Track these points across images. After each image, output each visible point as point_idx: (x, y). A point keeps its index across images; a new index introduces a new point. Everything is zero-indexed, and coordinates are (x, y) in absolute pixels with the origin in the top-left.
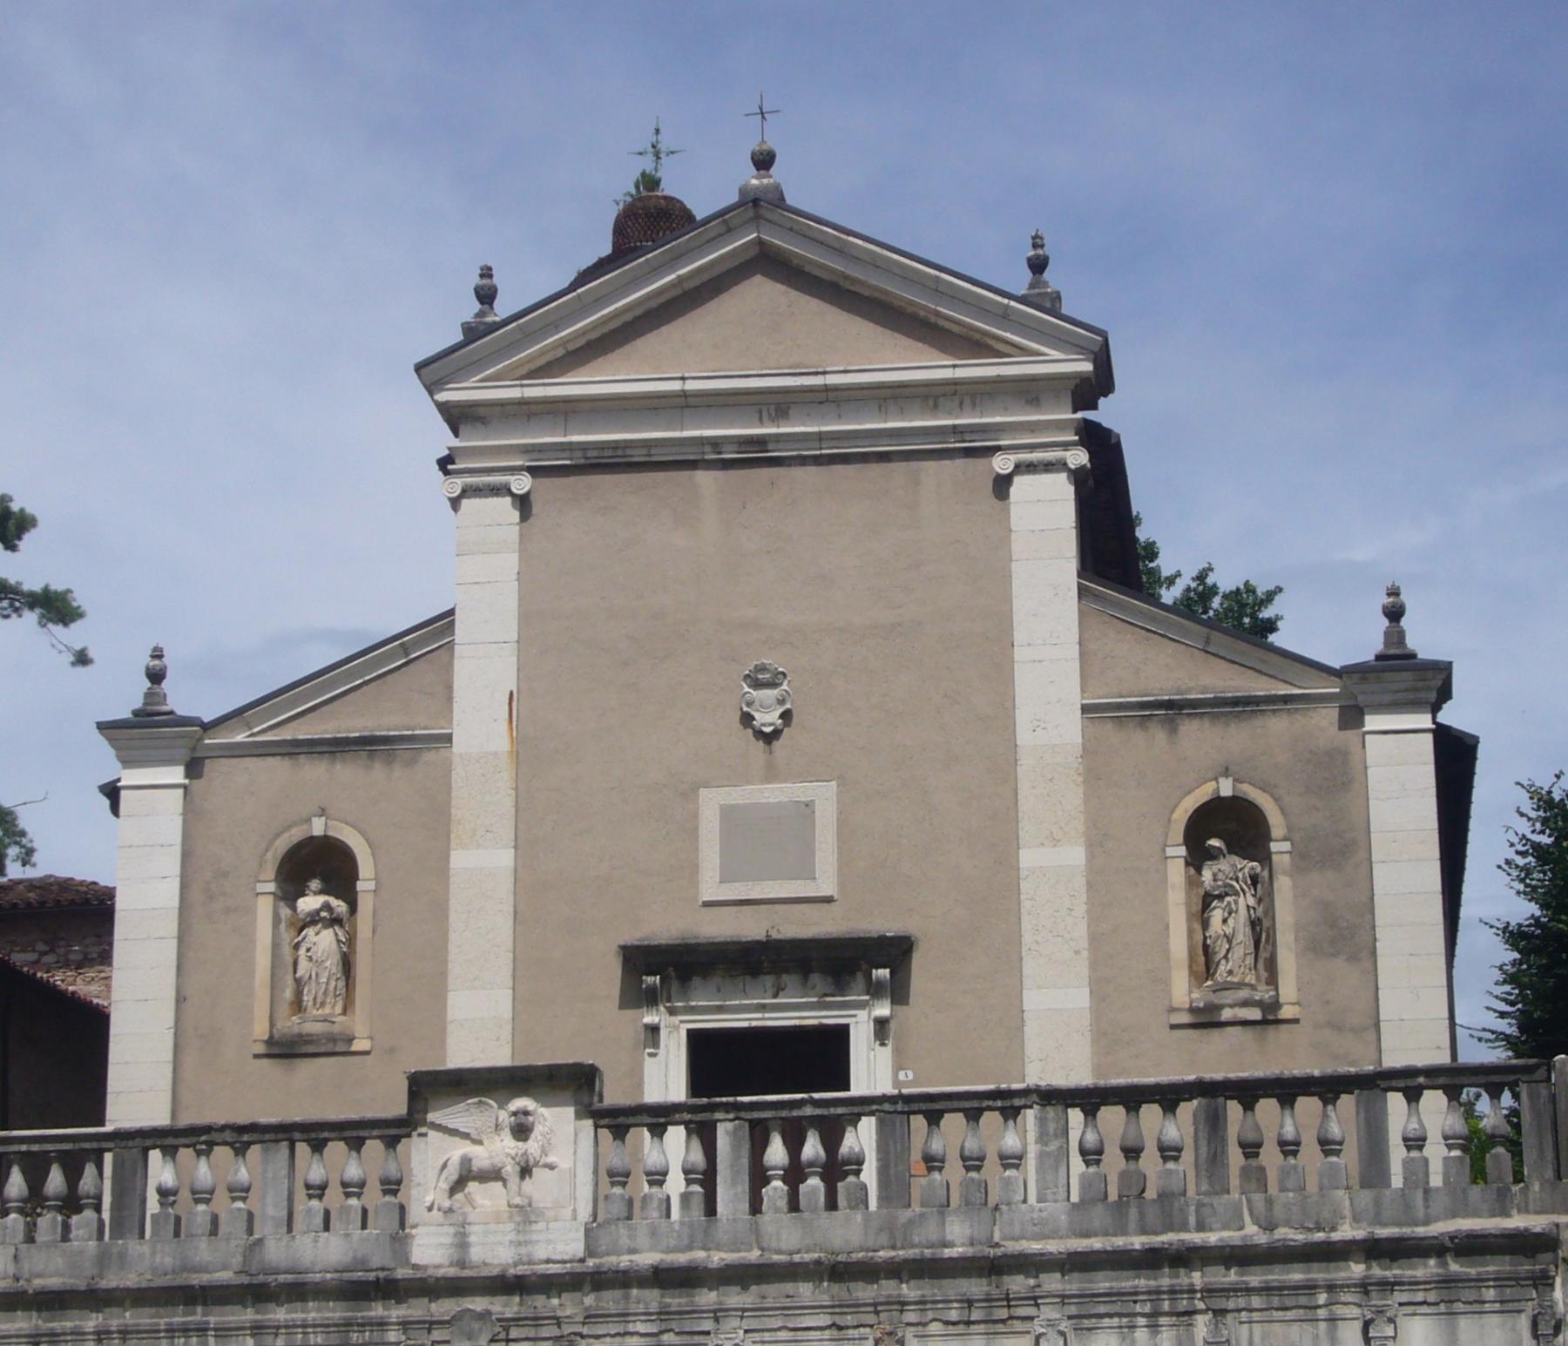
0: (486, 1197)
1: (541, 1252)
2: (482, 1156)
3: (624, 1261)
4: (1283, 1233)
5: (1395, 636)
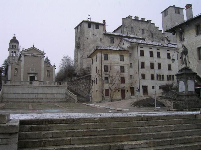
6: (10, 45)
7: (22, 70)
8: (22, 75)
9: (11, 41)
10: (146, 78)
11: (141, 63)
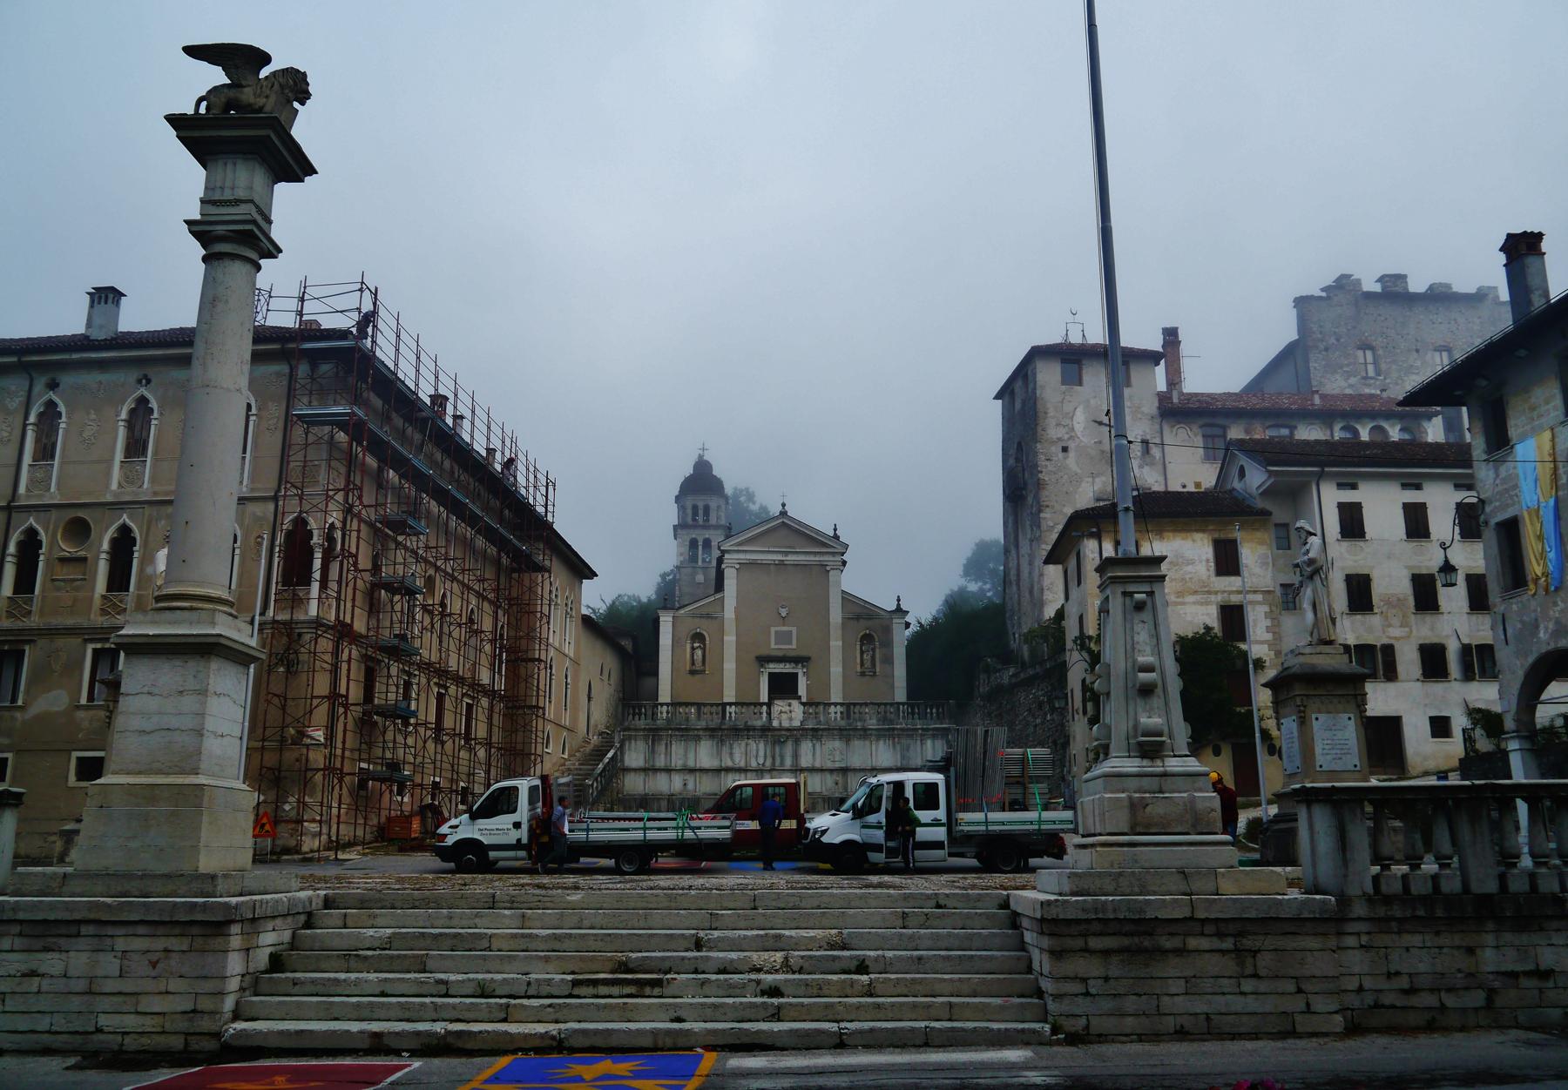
0: (784, 716)
2: (783, 710)
5: (899, 605)
6: (682, 508)
7: (730, 639)
8: (730, 666)
10: (1401, 669)
11: (1349, 579)
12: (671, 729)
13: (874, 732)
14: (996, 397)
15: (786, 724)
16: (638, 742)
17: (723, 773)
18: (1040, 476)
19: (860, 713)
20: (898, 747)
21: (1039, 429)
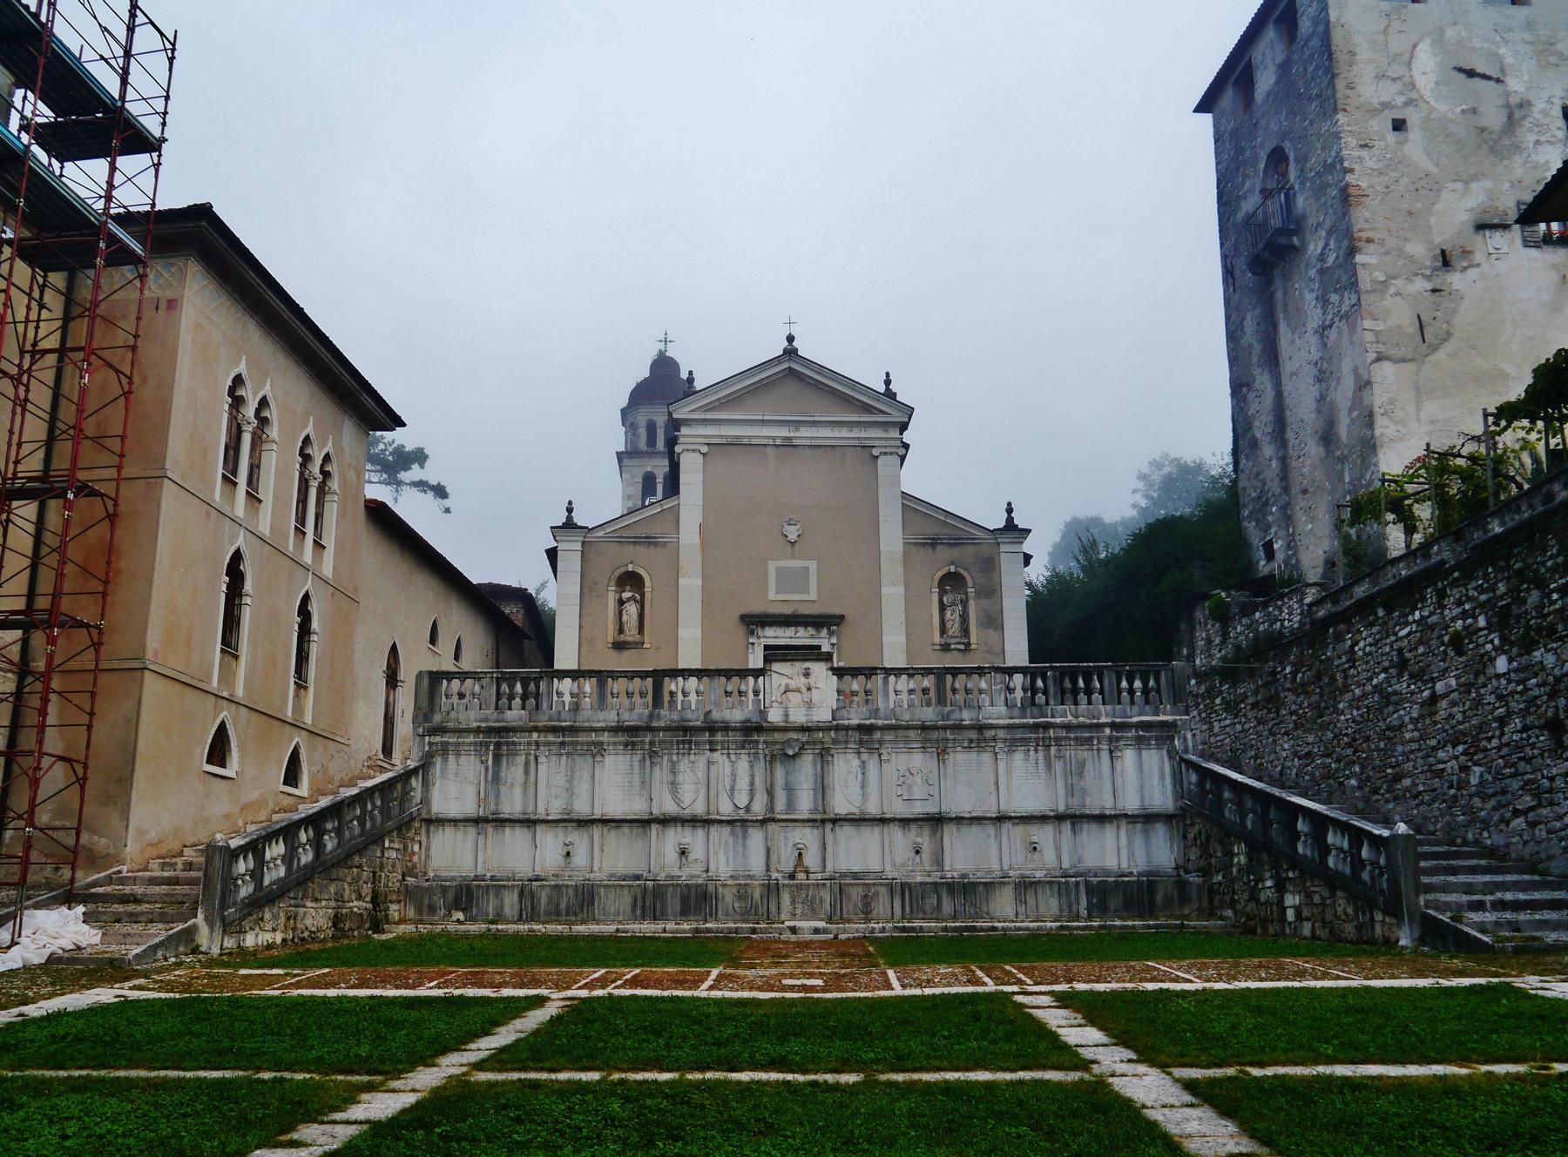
0: (794, 699)
1: (816, 718)
2: (793, 685)
3: (846, 722)
4: (1081, 719)
7: (691, 584)
9: (642, 395)
12: (536, 729)
13: (1001, 734)
14: (1202, 107)
15: (798, 717)
16: (463, 759)
17: (654, 827)
18: (1349, 178)
19: (968, 691)
20: (1058, 766)
21: (1340, 85)
